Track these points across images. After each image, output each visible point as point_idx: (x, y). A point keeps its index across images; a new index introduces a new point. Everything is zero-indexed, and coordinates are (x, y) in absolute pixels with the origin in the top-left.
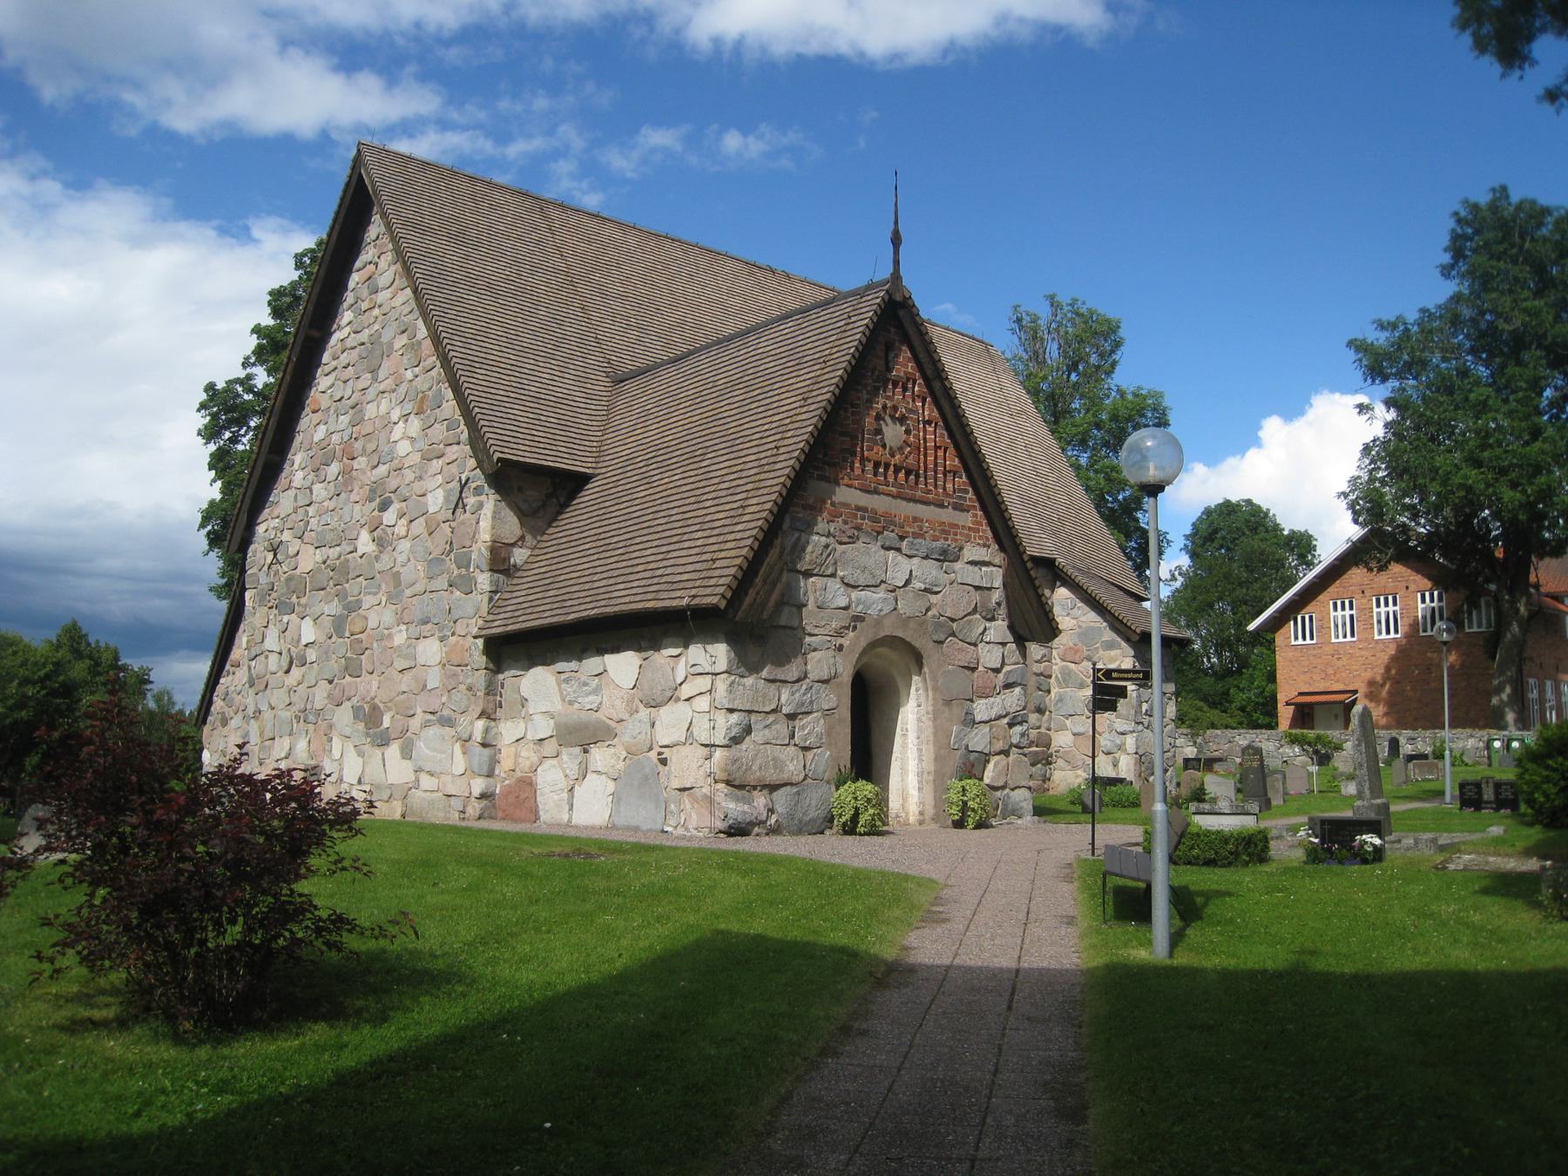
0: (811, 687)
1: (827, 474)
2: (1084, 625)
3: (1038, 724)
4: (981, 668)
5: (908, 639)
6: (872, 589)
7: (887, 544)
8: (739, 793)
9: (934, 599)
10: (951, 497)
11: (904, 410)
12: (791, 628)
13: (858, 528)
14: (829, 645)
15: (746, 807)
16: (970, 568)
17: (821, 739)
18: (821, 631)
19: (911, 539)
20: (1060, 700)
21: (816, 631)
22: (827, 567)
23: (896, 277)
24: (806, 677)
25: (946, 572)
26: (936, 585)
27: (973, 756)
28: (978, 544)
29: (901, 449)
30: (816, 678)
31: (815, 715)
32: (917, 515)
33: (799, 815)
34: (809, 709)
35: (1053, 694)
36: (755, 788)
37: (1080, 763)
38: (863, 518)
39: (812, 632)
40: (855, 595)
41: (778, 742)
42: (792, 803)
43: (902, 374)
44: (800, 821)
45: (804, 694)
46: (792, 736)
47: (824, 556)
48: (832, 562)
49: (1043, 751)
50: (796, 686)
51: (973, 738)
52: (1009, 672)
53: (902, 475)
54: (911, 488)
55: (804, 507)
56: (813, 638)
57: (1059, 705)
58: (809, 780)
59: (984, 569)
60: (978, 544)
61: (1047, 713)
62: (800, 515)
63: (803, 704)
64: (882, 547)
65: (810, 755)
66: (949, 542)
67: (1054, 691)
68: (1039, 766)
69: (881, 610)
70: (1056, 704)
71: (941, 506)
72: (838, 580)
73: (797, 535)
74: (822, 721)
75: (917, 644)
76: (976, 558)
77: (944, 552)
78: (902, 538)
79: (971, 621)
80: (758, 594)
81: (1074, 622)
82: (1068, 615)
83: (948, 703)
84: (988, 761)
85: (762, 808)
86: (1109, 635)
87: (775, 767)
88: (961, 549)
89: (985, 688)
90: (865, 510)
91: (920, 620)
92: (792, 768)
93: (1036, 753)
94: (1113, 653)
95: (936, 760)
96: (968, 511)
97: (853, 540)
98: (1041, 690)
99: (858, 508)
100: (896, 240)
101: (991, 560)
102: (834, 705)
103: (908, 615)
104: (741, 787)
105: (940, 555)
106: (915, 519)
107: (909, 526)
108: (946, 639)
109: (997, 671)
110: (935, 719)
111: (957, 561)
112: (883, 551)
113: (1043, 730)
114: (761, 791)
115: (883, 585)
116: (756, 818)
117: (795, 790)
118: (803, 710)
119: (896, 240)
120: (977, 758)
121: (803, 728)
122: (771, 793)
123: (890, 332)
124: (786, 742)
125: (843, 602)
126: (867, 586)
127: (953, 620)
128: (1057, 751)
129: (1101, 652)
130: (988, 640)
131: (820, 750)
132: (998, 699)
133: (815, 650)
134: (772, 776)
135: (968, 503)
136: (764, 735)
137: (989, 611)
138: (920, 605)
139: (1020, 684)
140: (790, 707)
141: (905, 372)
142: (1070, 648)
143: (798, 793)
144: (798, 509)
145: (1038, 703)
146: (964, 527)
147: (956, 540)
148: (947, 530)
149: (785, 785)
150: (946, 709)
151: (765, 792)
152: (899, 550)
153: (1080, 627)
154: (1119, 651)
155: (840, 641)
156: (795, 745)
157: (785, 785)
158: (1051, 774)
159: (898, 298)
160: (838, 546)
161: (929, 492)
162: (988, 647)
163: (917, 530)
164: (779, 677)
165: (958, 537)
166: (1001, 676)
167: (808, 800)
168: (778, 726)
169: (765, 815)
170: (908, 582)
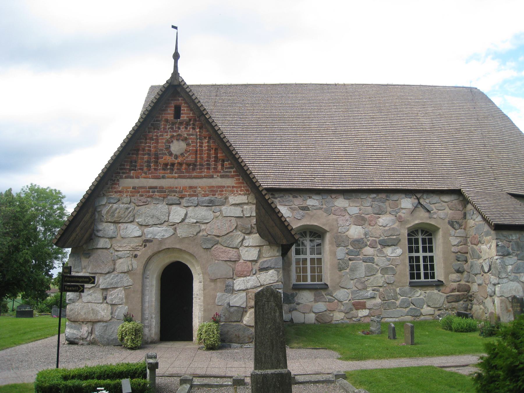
0: (117, 276)
1: (132, 175)
2: (477, 223)
3: (458, 279)
4: (241, 261)
5: (183, 249)
6: (158, 226)
7: (171, 202)
8: (73, 325)
9: (203, 227)
10: (220, 172)
11: (186, 135)
12: (106, 248)
13: (151, 197)
14: (129, 255)
15: (75, 332)
16: (233, 207)
17: (122, 300)
18: (124, 249)
19: (188, 198)
20: (472, 266)
21: (121, 249)
22: (129, 218)
23: (175, 73)
24: (114, 270)
25: (213, 212)
26: (204, 219)
27: (232, 309)
28: (240, 194)
29: (182, 154)
30: (121, 271)
31: (119, 289)
32: (191, 186)
33: (106, 337)
34: (116, 286)
35: (469, 262)
36: (83, 322)
37: (481, 301)
38: (154, 192)
39: (117, 250)
40: (146, 230)
41: (96, 302)
42: (103, 330)
43: (185, 118)
44: (108, 339)
45: (112, 279)
46: (105, 298)
47: (126, 213)
48: (132, 215)
49: (464, 295)
50: (107, 276)
51: (233, 299)
52: (264, 262)
53: (184, 166)
54: (189, 172)
55: (116, 192)
56: (119, 253)
57: (472, 269)
58: (113, 320)
59: (245, 207)
60: (240, 194)
61: (466, 273)
62: (114, 196)
63: (112, 284)
64: (167, 204)
65: (115, 308)
66: (216, 196)
67: (470, 261)
68: (461, 302)
69: (164, 236)
70: (471, 268)
71: (212, 177)
72: (136, 224)
73: (111, 205)
74: (123, 292)
75: (191, 252)
76: (237, 202)
77: (211, 201)
78: (182, 198)
79: (232, 236)
80: (77, 235)
81: (474, 222)
82: (472, 218)
83: (214, 281)
84: (246, 312)
85: (85, 332)
86: (486, 228)
87: (93, 313)
88: (226, 198)
89: (244, 271)
90: (156, 188)
91: (192, 239)
92: (103, 314)
93: (458, 295)
94: (488, 238)
95: (205, 311)
96: (234, 178)
97: (146, 203)
98: (459, 261)
99: (151, 188)
100: (176, 56)
101: (251, 201)
102: (131, 284)
103: (183, 236)
104: (74, 322)
105: (209, 203)
106: (191, 187)
107: (187, 192)
108: (212, 247)
109: (256, 261)
110: (204, 289)
111: (223, 204)
112: (167, 206)
113: (463, 282)
114: (86, 324)
115: (166, 224)
116: (80, 336)
117: (105, 324)
118: (112, 286)
119: (176, 56)
120: (236, 310)
121: (111, 295)
122: (93, 325)
123: (178, 100)
124: (101, 301)
125: (138, 233)
126: (155, 225)
127: (218, 236)
128: (473, 294)
129: (484, 238)
130: (247, 245)
131: (121, 306)
132: (254, 277)
133: (120, 258)
134: (91, 317)
135: (232, 174)
136: (87, 299)
137: (247, 229)
138: (194, 231)
139: (273, 268)
140: (103, 285)
141: (187, 117)
142: (473, 237)
143: (107, 326)
144: (112, 194)
145: (457, 268)
146: (228, 187)
147: (222, 195)
148: (213, 190)
149: (99, 321)
150: (212, 284)
151: (89, 324)
152: (179, 204)
153: (476, 224)
154: (490, 237)
155: (136, 253)
156: (107, 303)
157: (99, 321)
158: (472, 307)
159: (176, 83)
160: (137, 208)
161: (201, 172)
162: (246, 249)
163: (192, 193)
164: (98, 271)
165: (224, 192)
166: (258, 264)
167: (113, 329)
168: (96, 295)
169: (86, 335)
170: (183, 220)
